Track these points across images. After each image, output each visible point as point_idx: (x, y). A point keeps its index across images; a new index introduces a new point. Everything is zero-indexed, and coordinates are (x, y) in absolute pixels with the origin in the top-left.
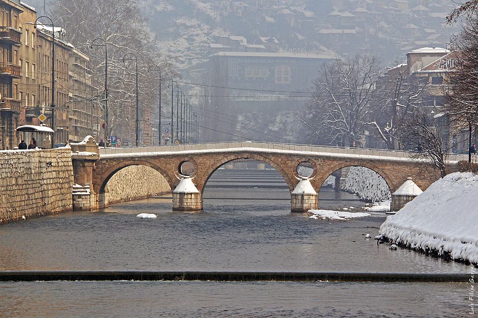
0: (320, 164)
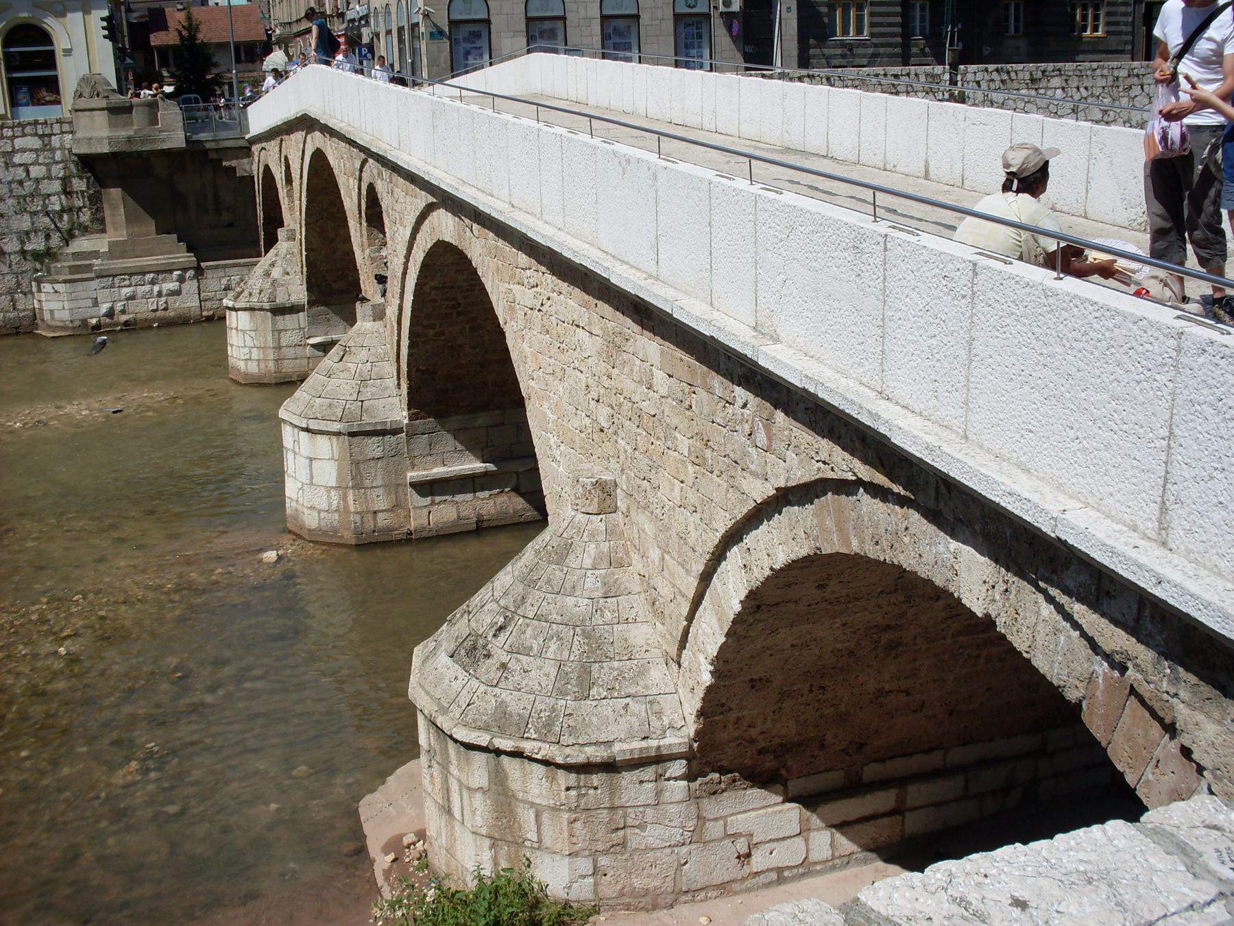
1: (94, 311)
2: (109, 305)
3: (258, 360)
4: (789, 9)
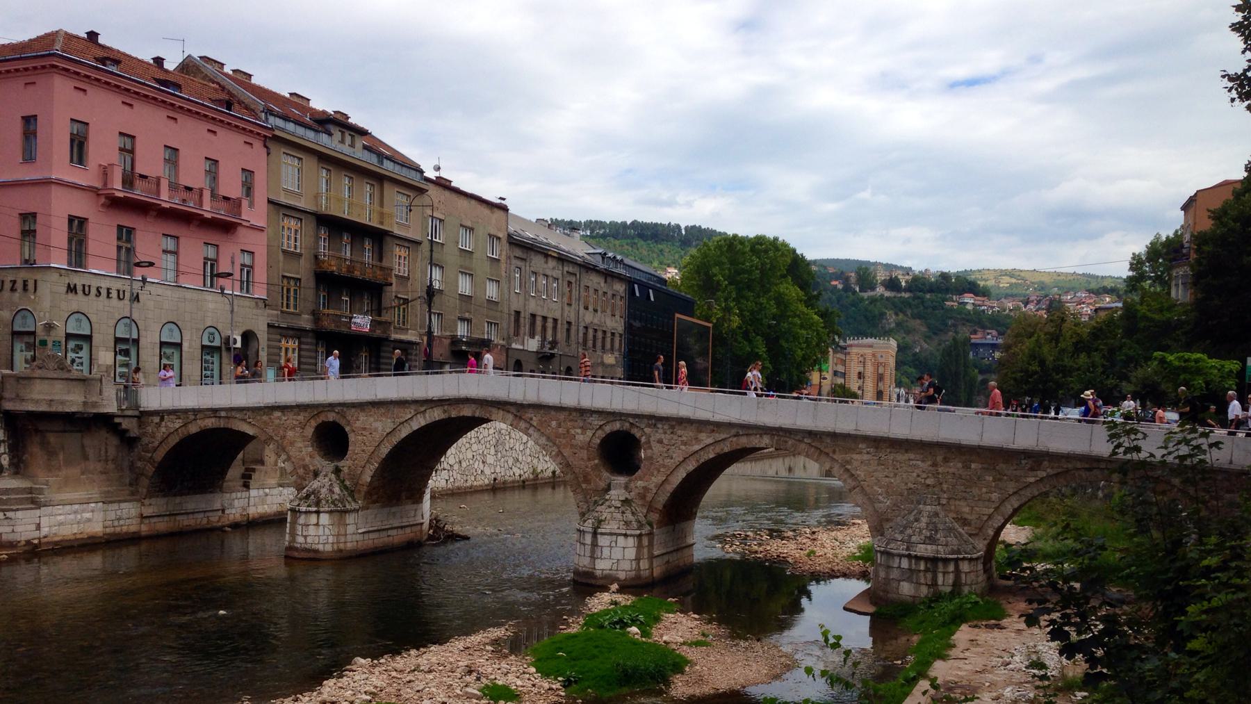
1: (36, 534)
2: (47, 529)
3: (333, 543)
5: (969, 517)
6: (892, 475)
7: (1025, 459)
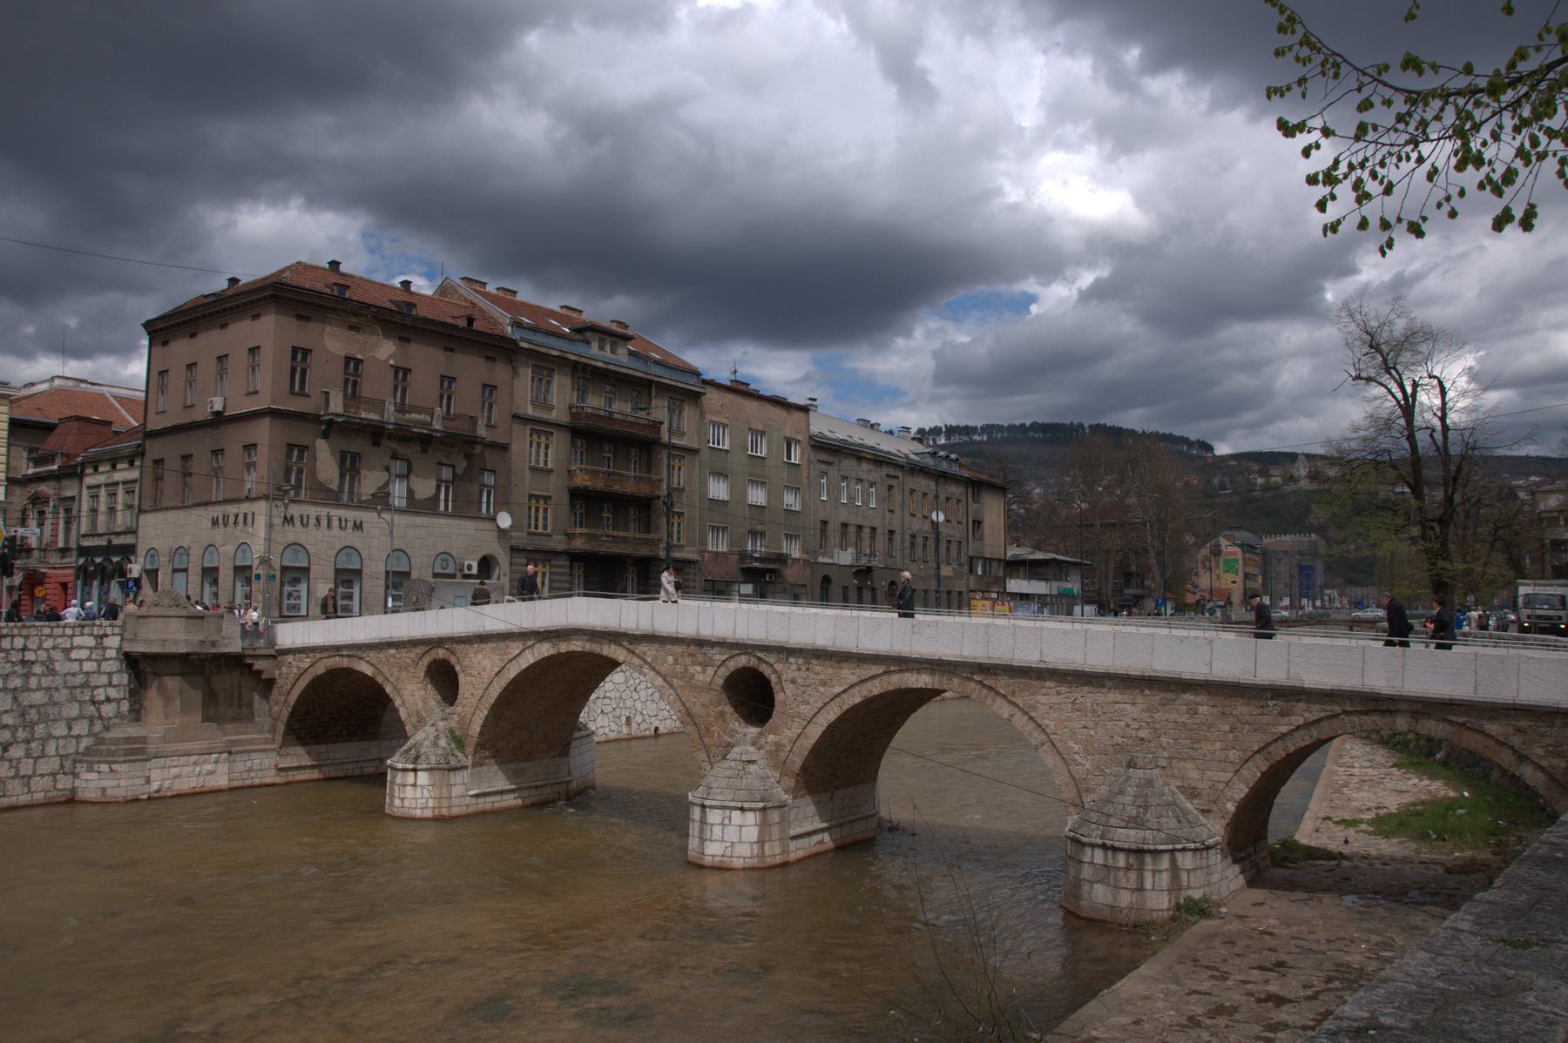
0: (793, 681)
2: (158, 783)
3: (433, 808)
4: (505, 574)
5: (1199, 785)
6: (1091, 725)
7: (1272, 699)
